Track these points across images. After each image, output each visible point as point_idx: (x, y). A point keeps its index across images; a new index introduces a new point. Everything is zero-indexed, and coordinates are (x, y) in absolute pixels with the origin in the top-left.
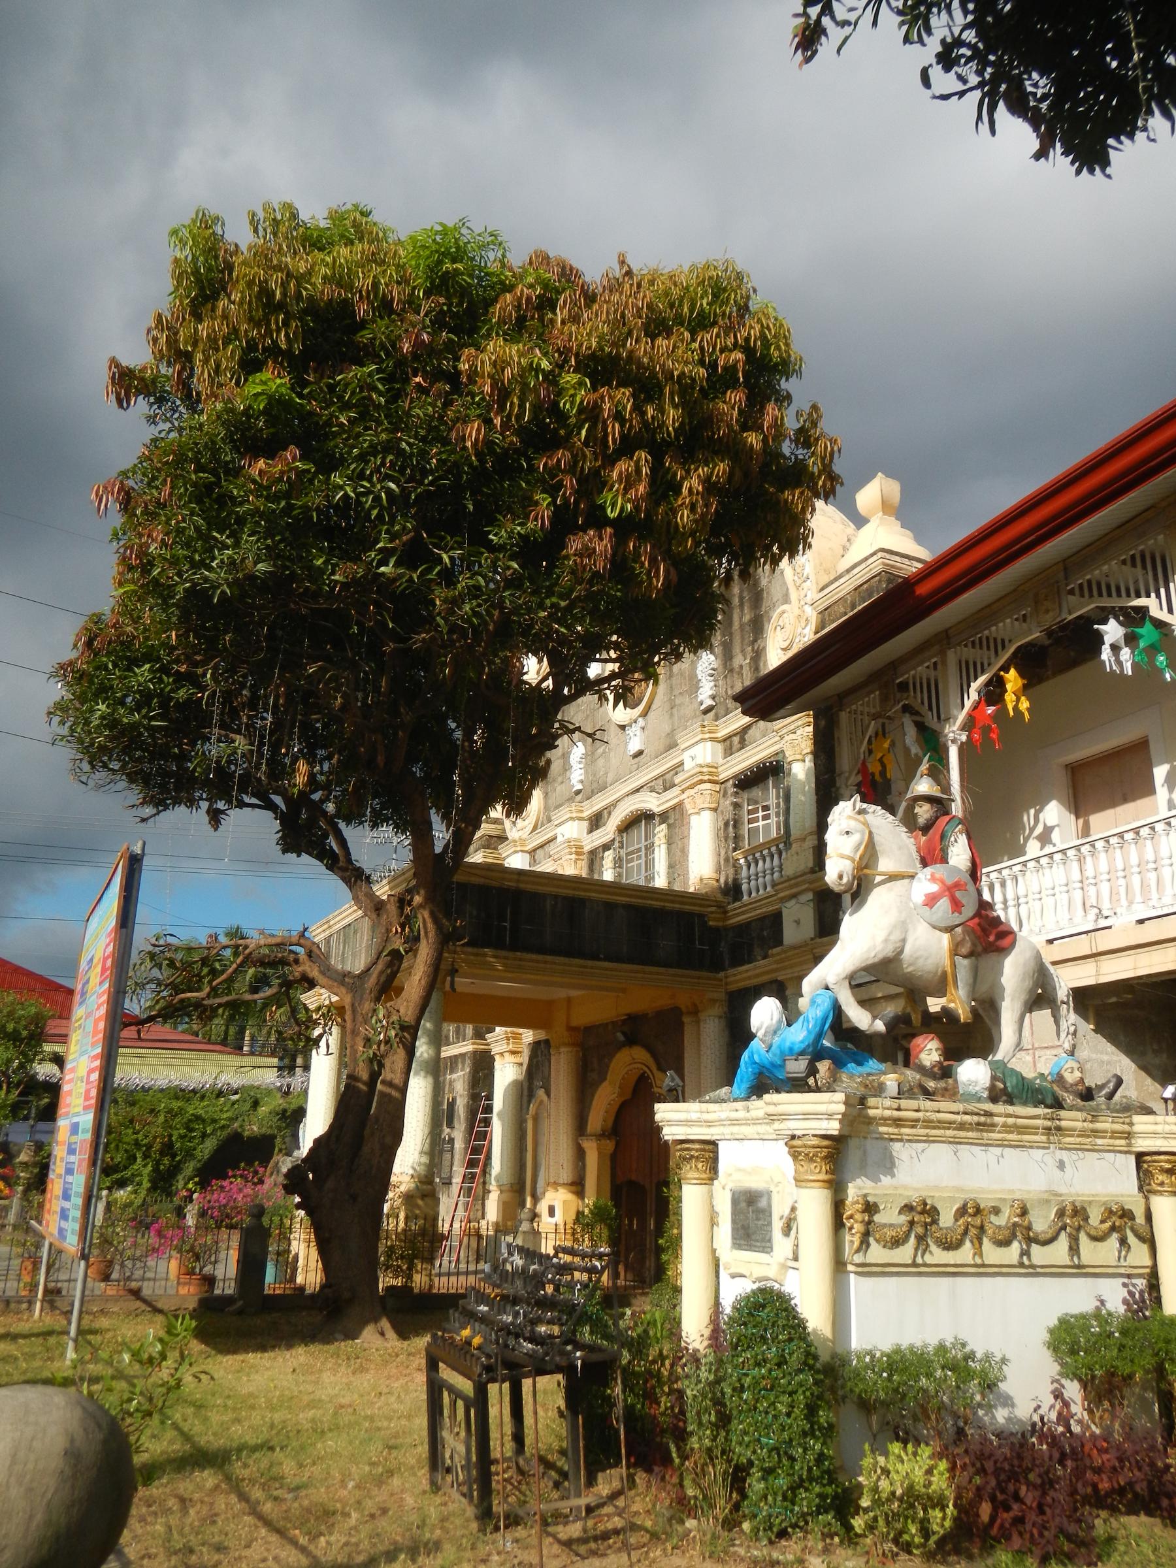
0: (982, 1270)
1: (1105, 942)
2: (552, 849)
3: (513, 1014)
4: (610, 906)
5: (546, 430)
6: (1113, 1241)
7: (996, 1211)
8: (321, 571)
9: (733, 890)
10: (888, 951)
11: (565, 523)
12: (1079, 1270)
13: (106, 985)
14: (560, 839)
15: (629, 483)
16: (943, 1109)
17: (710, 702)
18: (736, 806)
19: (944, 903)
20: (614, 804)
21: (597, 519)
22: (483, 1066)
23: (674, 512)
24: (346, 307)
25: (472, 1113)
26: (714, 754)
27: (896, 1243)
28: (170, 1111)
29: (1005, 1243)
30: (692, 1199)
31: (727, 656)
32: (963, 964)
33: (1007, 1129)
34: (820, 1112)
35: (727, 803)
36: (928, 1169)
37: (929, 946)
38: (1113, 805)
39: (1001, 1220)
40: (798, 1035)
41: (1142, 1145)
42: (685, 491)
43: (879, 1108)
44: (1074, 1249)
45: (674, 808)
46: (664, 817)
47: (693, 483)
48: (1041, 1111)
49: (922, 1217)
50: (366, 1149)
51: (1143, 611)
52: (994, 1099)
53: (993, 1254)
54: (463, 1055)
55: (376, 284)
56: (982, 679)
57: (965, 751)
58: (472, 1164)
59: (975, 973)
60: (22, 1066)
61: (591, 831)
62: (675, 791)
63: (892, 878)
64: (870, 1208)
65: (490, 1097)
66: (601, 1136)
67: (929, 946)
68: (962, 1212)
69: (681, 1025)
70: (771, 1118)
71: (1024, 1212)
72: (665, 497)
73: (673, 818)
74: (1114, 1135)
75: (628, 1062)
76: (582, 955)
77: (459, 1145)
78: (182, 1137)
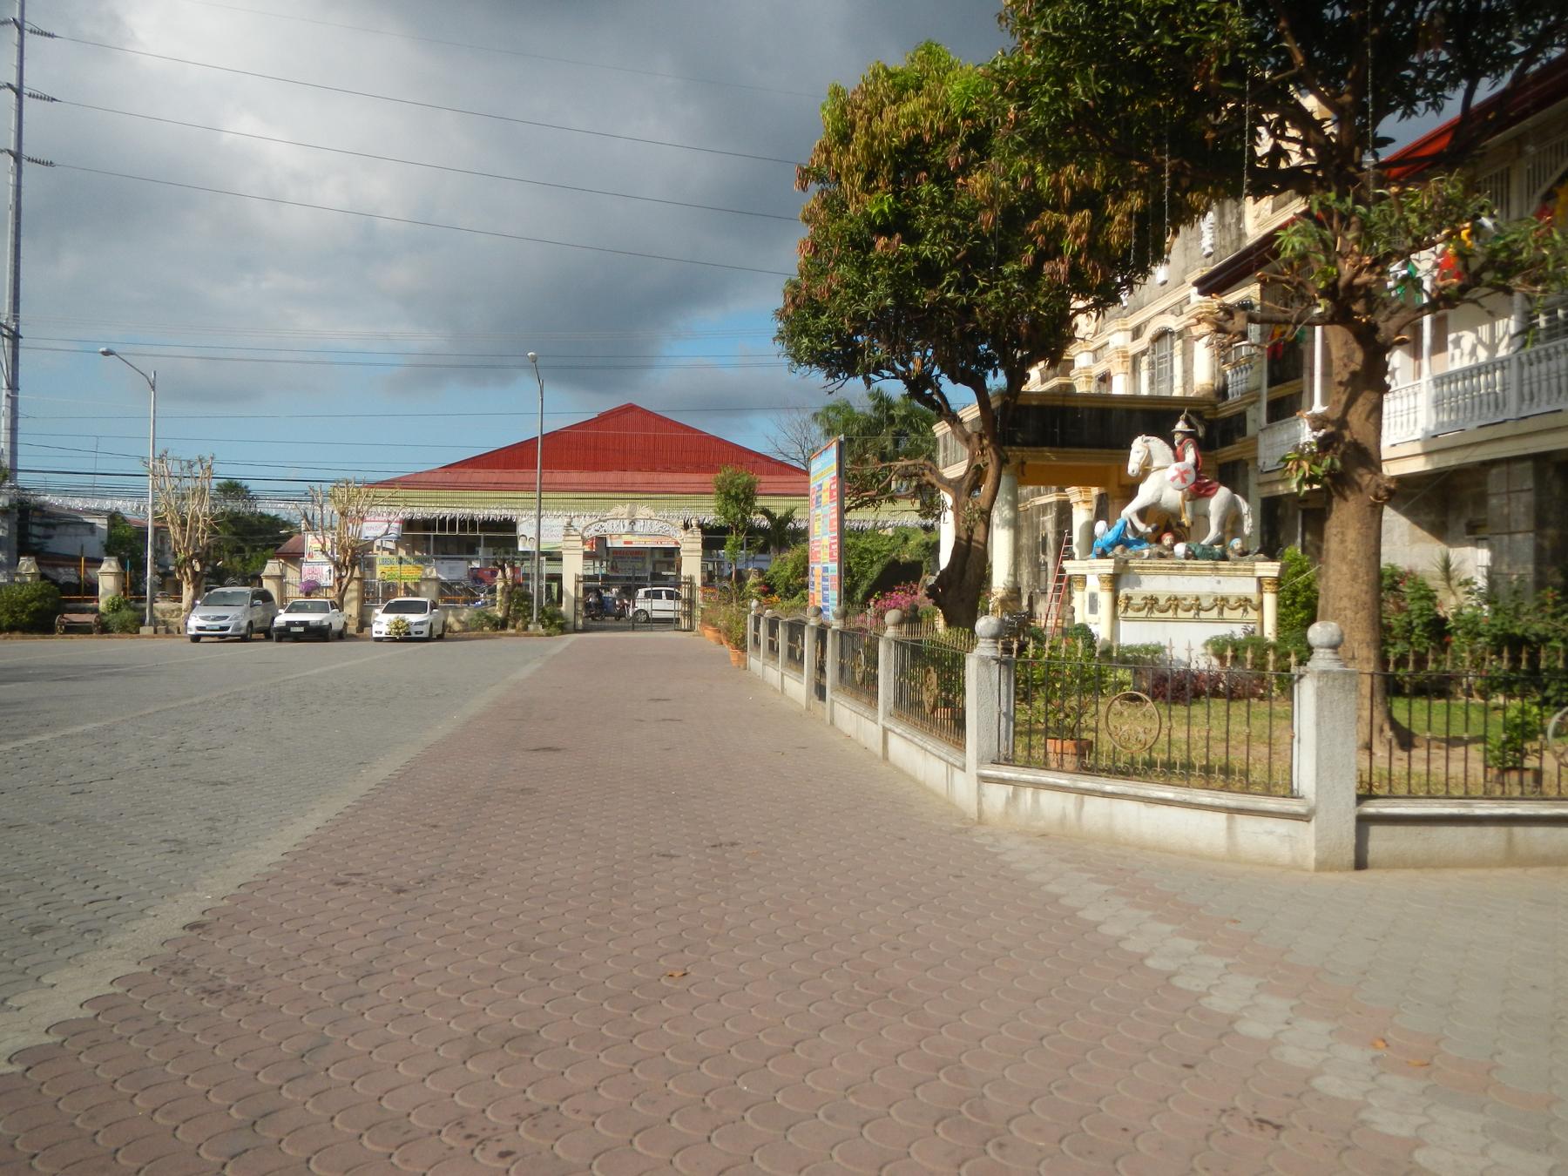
0: (1176, 620)
4: (1130, 412)
9: (1222, 392)
12: (1223, 621)
14: (1111, 346)
15: (1077, 234)
17: (1209, 250)
19: (1179, 480)
20: (1148, 321)
22: (1064, 513)
24: (918, 139)
25: (1059, 544)
27: (1139, 610)
31: (1221, 216)
40: (1111, 536)
41: (1259, 574)
43: (1133, 563)
44: (1221, 612)
46: (1180, 334)
49: (1151, 602)
50: (967, 577)
52: (1187, 557)
60: (743, 519)
61: (1134, 339)
62: (1183, 318)
64: (1128, 598)
65: (1070, 533)
71: (1197, 599)
77: (1050, 566)
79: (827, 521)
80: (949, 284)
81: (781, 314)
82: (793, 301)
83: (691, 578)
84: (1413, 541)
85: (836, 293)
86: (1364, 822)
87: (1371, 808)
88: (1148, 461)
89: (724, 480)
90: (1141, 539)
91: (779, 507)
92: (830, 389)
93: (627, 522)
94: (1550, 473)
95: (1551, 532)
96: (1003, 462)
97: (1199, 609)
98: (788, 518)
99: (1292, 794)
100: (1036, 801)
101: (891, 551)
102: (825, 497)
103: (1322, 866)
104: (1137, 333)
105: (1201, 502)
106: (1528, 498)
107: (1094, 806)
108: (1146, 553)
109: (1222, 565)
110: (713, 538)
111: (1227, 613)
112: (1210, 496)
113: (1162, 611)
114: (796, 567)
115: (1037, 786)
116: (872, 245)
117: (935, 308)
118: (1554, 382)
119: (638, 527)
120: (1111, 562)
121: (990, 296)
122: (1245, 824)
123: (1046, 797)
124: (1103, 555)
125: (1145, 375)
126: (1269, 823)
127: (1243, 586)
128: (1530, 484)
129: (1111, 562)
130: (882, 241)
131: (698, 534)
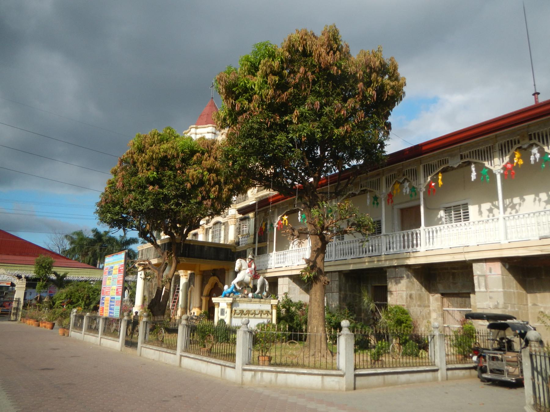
3: (186, 268)
4: (210, 247)
5: (201, 183)
9: (238, 243)
11: (203, 198)
12: (261, 318)
13: (122, 274)
15: (215, 192)
16: (246, 299)
18: (240, 224)
24: (166, 156)
28: (89, 288)
30: (216, 309)
34: (230, 300)
35: (238, 223)
36: (243, 306)
37: (248, 278)
40: (229, 290)
41: (272, 303)
43: (237, 299)
44: (261, 315)
46: (224, 224)
47: (226, 189)
49: (242, 312)
52: (252, 298)
53: (250, 316)
57: (277, 228)
58: (174, 302)
64: (235, 311)
65: (179, 286)
66: (206, 296)
67: (248, 278)
69: (225, 273)
73: (226, 224)
75: (213, 280)
78: (92, 294)
79: (116, 280)
80: (173, 203)
81: (99, 204)
82: (105, 201)
83: (19, 299)
84: (300, 294)
85: (131, 202)
86: (356, 376)
87: (358, 372)
88: (241, 266)
90: (237, 291)
91: (61, 271)
94: (342, 276)
95: (343, 292)
96: (178, 262)
97: (255, 314)
98: (65, 276)
99: (338, 369)
100: (262, 376)
102: (115, 272)
103: (347, 389)
105: (255, 280)
106: (337, 283)
107: (281, 376)
108: (240, 296)
109: (262, 300)
110: (31, 283)
111: (263, 316)
112: (258, 279)
114: (67, 295)
115: (262, 371)
116: (146, 187)
117: (168, 211)
120: (231, 299)
121: (185, 209)
122: (327, 379)
123: (265, 374)
124: (229, 297)
125: (210, 235)
126: (333, 378)
127: (266, 307)
128: (337, 279)
129: (231, 299)
130: (151, 187)
131: (24, 282)
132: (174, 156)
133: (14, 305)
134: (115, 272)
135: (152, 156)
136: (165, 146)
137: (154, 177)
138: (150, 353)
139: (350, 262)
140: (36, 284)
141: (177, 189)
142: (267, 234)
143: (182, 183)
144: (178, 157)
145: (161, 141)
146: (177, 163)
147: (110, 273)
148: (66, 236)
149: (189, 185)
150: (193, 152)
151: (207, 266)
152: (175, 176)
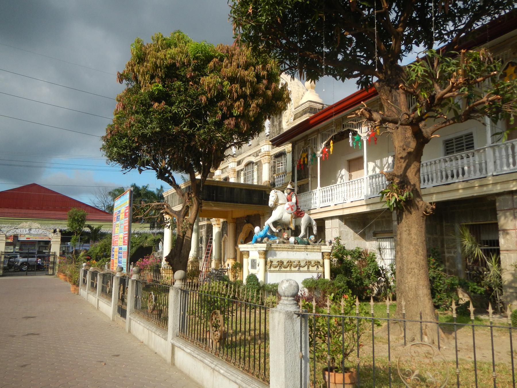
0: (291, 271)
1: (345, 206)
2: (227, 170)
3: (217, 215)
5: (221, 96)
6: (316, 267)
7: (294, 262)
8: (171, 129)
10: (279, 218)
11: (225, 117)
12: (309, 271)
13: (127, 219)
14: (229, 167)
17: (268, 134)
18: (274, 162)
19: (290, 209)
20: (244, 159)
21: (232, 115)
22: (210, 228)
23: (249, 111)
24: (174, 65)
26: (269, 148)
27: (276, 267)
29: (296, 267)
30: (245, 260)
31: (273, 122)
32: (293, 220)
33: (297, 248)
34: (263, 247)
35: (272, 161)
36: (283, 255)
37: (287, 217)
38: (357, 171)
39: (295, 264)
40: (262, 233)
41: (323, 251)
42: (252, 106)
43: (274, 246)
44: (308, 268)
45: (259, 161)
46: (256, 163)
47: (253, 105)
48: (304, 245)
49: (281, 263)
51: (356, 132)
52: (295, 243)
54: (204, 225)
55: (181, 59)
56: (325, 142)
57: (321, 158)
58: (207, 253)
59: (295, 221)
61: (238, 165)
62: (259, 157)
63: (281, 204)
64: (271, 262)
65: (212, 236)
67: (287, 217)
68: (288, 262)
69: (260, 219)
70: (255, 248)
71: (299, 262)
72: (248, 107)
73: (259, 164)
74: (317, 249)
76: (234, 202)
77: (204, 248)
79: (122, 227)
80: (185, 125)
83: (55, 253)
84: (355, 239)
85: (133, 125)
89: (72, 213)
91: (95, 225)
92: (125, 172)
93: (27, 230)
96: (200, 205)
97: (300, 267)
101: (140, 242)
102: (122, 216)
104: (239, 163)
105: (298, 219)
108: (278, 241)
109: (309, 247)
110: (66, 237)
111: (311, 268)
112: (302, 217)
113: (285, 268)
114: (101, 249)
118: (439, 174)
119: (32, 232)
120: (265, 245)
121: (202, 131)
124: (261, 242)
129: (265, 245)
130: (156, 104)
131: (59, 235)
132: (184, 63)
133: (51, 259)
134: (122, 216)
135: (156, 63)
136: (173, 51)
137: (159, 90)
138: (140, 328)
139: (432, 191)
140: (71, 238)
141: (191, 106)
142: (308, 169)
143: (195, 97)
144: (190, 65)
145: (169, 46)
146: (189, 73)
147: (118, 219)
148: (110, 193)
149: (204, 98)
150: (209, 58)
151: (240, 211)
152: (186, 89)
